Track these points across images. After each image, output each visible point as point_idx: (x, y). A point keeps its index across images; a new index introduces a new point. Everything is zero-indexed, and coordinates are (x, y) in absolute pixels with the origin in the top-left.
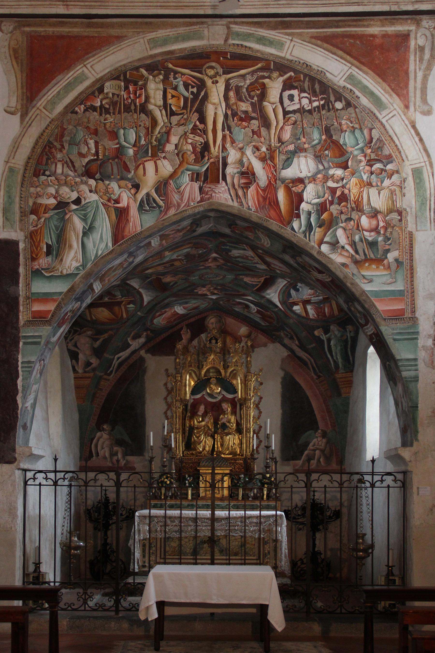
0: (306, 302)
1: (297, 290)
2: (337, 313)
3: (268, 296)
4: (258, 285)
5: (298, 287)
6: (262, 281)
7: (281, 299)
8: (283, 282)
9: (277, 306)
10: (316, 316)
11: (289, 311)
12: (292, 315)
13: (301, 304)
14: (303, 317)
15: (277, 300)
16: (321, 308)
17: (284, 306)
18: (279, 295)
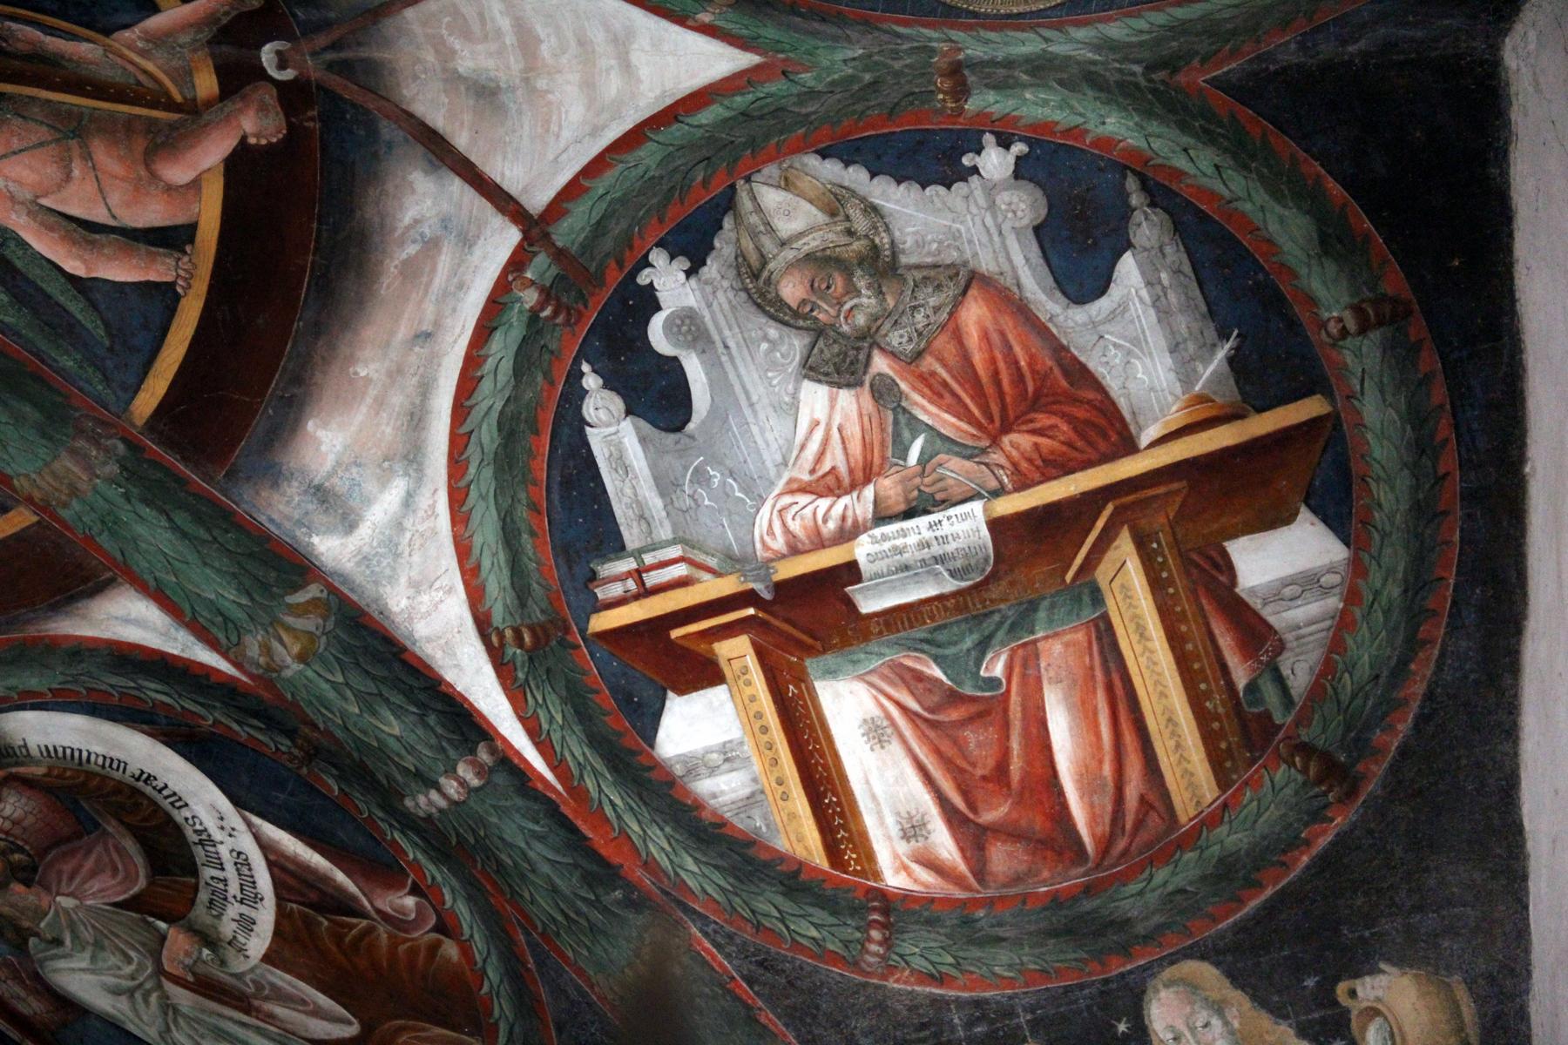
0: (807, 615)
1: (660, 398)
2: (1209, 790)
3: (331, 549)
4: (165, 297)
5: (658, 335)
6: (209, 214)
7: (496, 585)
8: (467, 241)
9: (465, 724)
10: (944, 843)
11: (612, 796)
12: (658, 843)
13: (737, 652)
14: (795, 881)
15: (456, 607)
16: (988, 708)
17: (555, 713)
18: (457, 498)
